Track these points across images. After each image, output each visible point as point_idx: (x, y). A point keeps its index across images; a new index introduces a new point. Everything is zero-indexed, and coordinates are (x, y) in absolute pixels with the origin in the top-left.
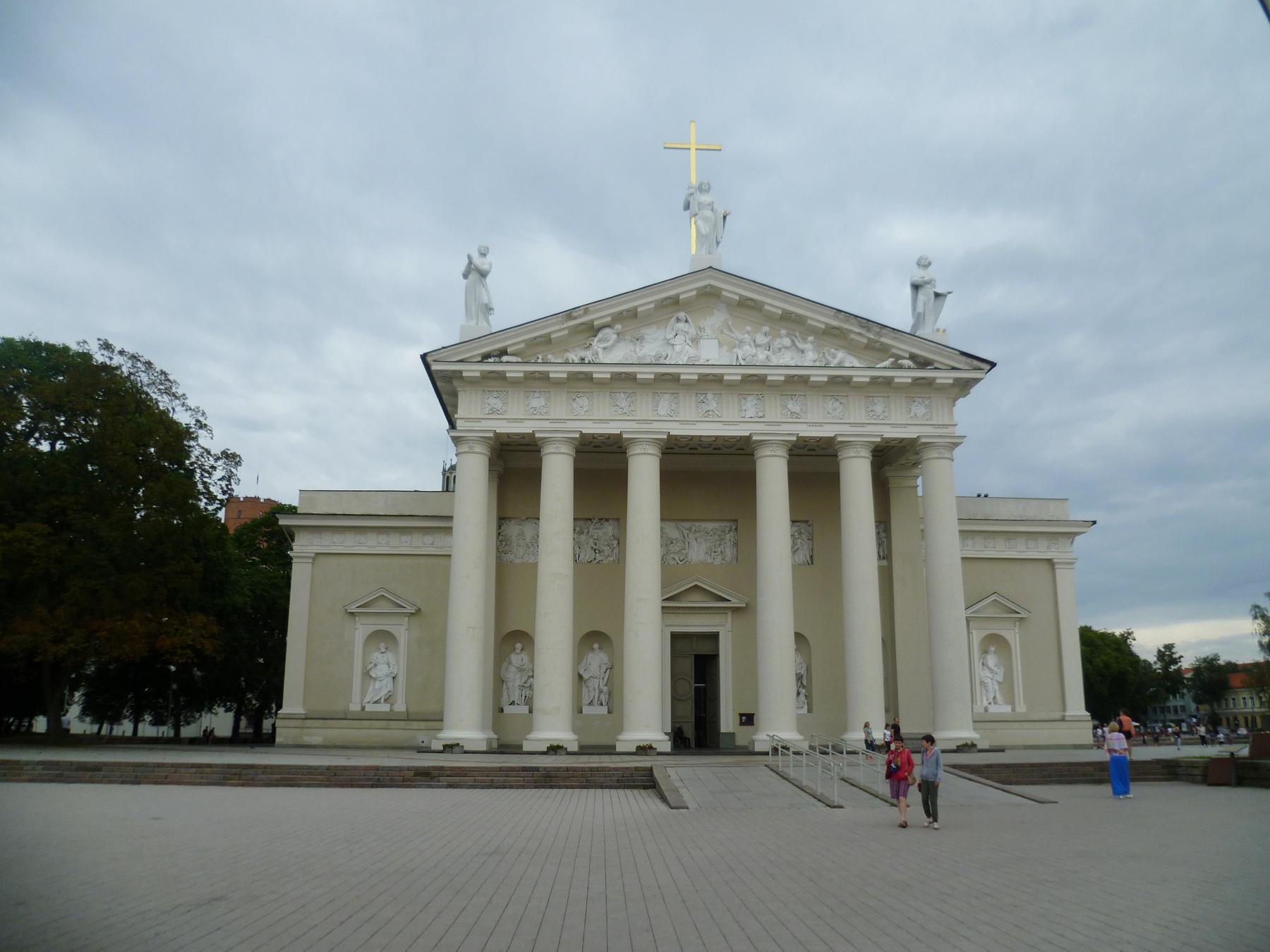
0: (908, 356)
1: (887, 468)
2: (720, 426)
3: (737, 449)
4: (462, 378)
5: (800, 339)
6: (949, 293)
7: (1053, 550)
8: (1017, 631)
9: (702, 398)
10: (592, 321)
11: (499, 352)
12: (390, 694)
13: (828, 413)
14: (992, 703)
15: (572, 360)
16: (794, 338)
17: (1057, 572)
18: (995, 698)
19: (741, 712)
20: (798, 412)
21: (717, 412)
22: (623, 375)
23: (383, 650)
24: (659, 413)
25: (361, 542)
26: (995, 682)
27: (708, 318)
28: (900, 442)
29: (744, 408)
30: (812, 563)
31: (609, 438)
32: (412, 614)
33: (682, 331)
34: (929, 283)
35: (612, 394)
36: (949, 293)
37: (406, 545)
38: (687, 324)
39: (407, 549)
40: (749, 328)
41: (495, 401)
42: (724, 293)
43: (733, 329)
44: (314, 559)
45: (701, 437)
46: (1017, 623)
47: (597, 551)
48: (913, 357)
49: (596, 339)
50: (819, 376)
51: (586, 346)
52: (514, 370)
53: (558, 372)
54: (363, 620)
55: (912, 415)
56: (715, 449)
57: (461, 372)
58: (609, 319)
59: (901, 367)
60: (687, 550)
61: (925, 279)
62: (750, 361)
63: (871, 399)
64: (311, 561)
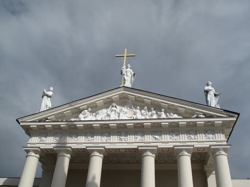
1: (205, 166)
2: (126, 144)
5: (159, 110)
13: (171, 138)
16: (157, 111)
22: (88, 125)
28: (204, 150)
38: (116, 108)
40: (138, 107)
45: (119, 149)
48: (204, 114)
49: (81, 114)
52: (48, 125)
57: (30, 125)
59: (200, 118)
62: (139, 118)
63: (189, 132)
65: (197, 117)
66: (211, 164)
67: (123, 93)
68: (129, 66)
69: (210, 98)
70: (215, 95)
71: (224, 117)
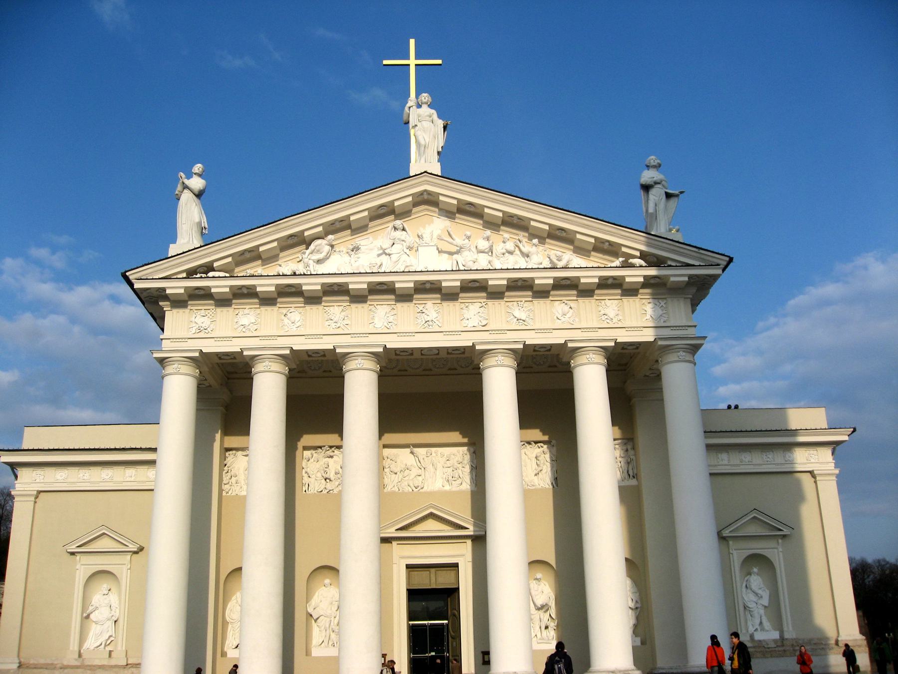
0: (638, 254)
3: (473, 369)
4: (166, 298)
6: (682, 193)
7: (812, 461)
8: (780, 550)
11: (206, 269)
12: (112, 639)
13: (558, 319)
14: (759, 630)
15: (283, 273)
18: (761, 623)
19: (483, 650)
21: (437, 322)
23: (106, 592)
24: (375, 326)
25: (85, 478)
26: (760, 607)
27: (427, 226)
28: (637, 348)
29: (466, 316)
30: (557, 486)
31: (324, 356)
33: (398, 239)
34: (659, 183)
35: (325, 308)
36: (682, 193)
37: (128, 479)
39: (129, 484)
41: (203, 319)
42: (441, 198)
43: (454, 236)
44: (37, 497)
45: (422, 349)
46: (780, 541)
47: (327, 480)
49: (308, 252)
51: (298, 260)
52: (220, 285)
53: (266, 286)
54: (85, 559)
56: (450, 369)
57: (164, 289)
58: (320, 229)
59: (632, 266)
60: (423, 476)
61: (655, 179)
64: (33, 499)
65: (626, 265)
66: (648, 376)
67: (425, 191)
68: (425, 97)
69: (656, 205)
70: (668, 196)
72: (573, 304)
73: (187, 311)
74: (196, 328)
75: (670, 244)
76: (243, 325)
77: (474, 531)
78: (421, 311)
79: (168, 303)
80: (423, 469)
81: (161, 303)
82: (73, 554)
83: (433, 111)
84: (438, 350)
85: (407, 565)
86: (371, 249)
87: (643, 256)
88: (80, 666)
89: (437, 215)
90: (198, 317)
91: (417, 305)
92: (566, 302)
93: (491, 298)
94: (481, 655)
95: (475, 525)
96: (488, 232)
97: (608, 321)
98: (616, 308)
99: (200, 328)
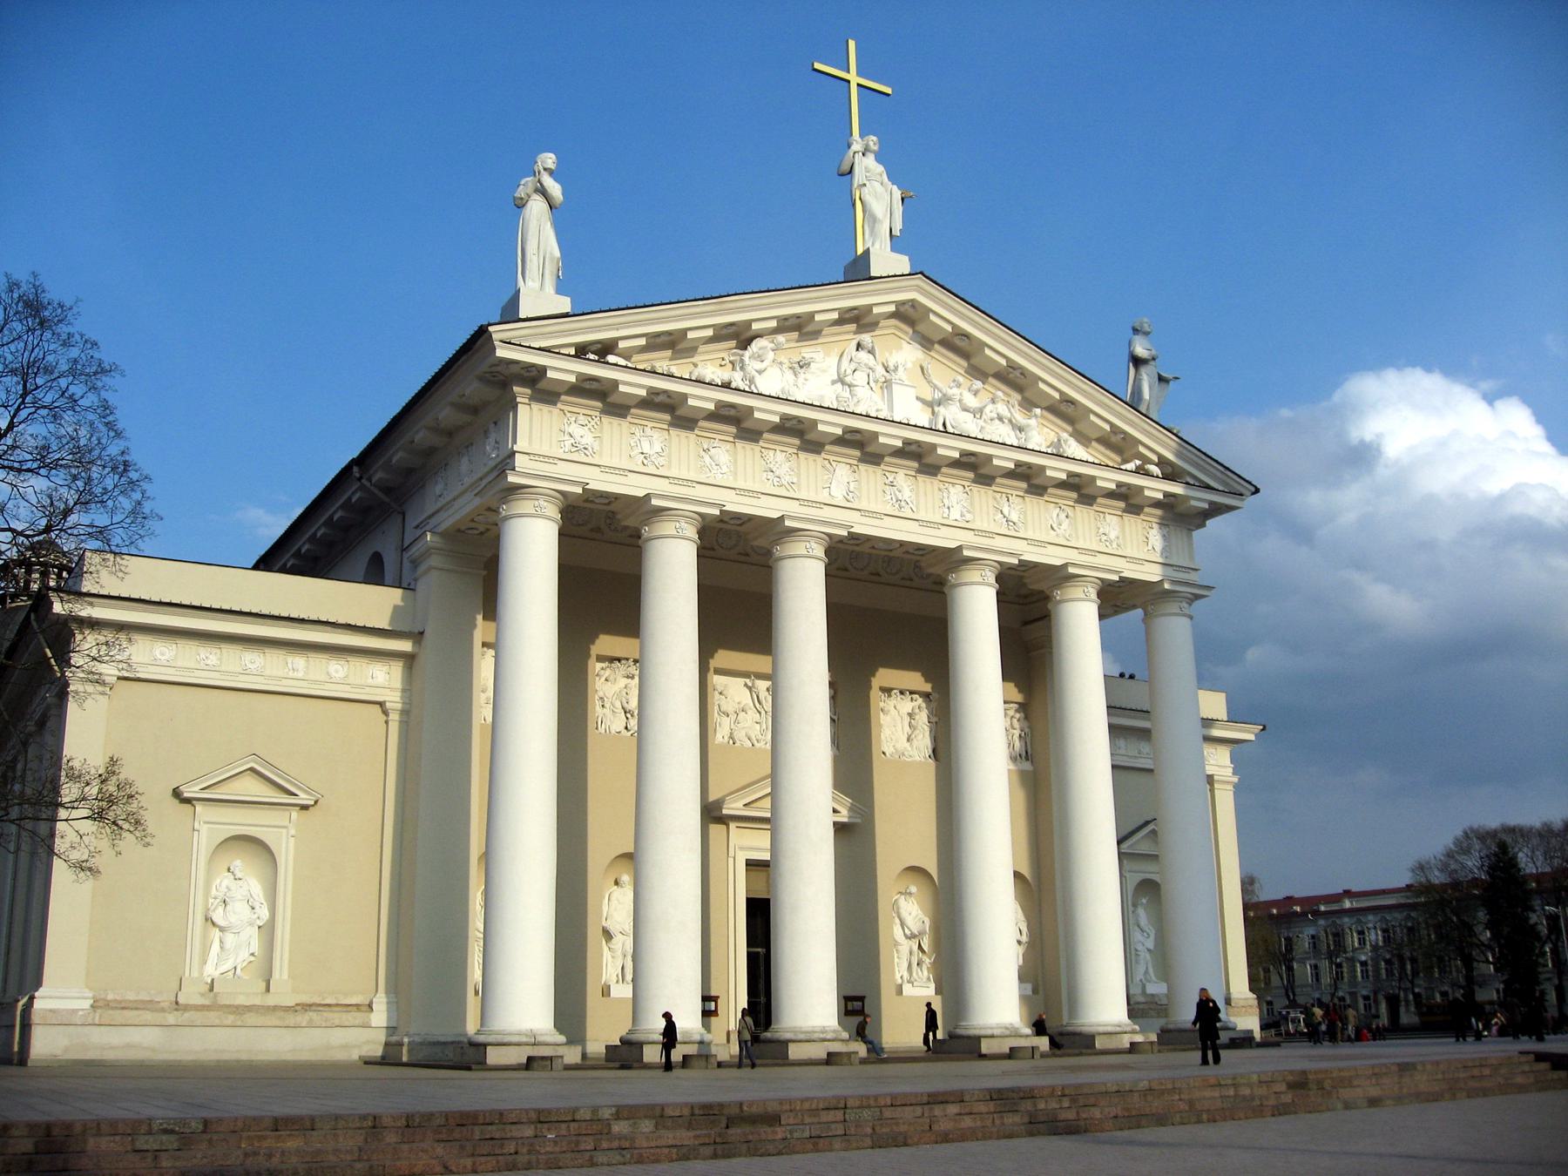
0: (1156, 460)
9: (891, 479)
10: (749, 323)
11: (599, 346)
17: (1216, 791)
20: (1015, 520)
25: (209, 662)
27: (894, 351)
32: (305, 807)
33: (865, 365)
35: (763, 450)
37: (295, 675)
38: (871, 356)
42: (932, 317)
50: (1057, 470)
52: (633, 385)
55: (1150, 548)
57: (542, 370)
59: (1148, 474)
65: (1140, 471)
68: (872, 140)
70: (1161, 379)
71: (1218, 490)
72: (1070, 510)
73: (555, 411)
74: (570, 442)
75: (1197, 456)
76: (642, 453)
77: (849, 817)
78: (892, 482)
79: (528, 391)
80: (763, 712)
81: (516, 389)
82: (188, 801)
83: (881, 168)
84: (901, 545)
85: (746, 860)
86: (824, 371)
87: (1162, 462)
88: (208, 1006)
89: (908, 340)
90: (573, 425)
91: (887, 473)
92: (1063, 507)
93: (1032, 493)
94: (843, 1001)
95: (851, 809)
96: (978, 384)
97: (1108, 544)
98: (1117, 527)
99: (577, 445)
